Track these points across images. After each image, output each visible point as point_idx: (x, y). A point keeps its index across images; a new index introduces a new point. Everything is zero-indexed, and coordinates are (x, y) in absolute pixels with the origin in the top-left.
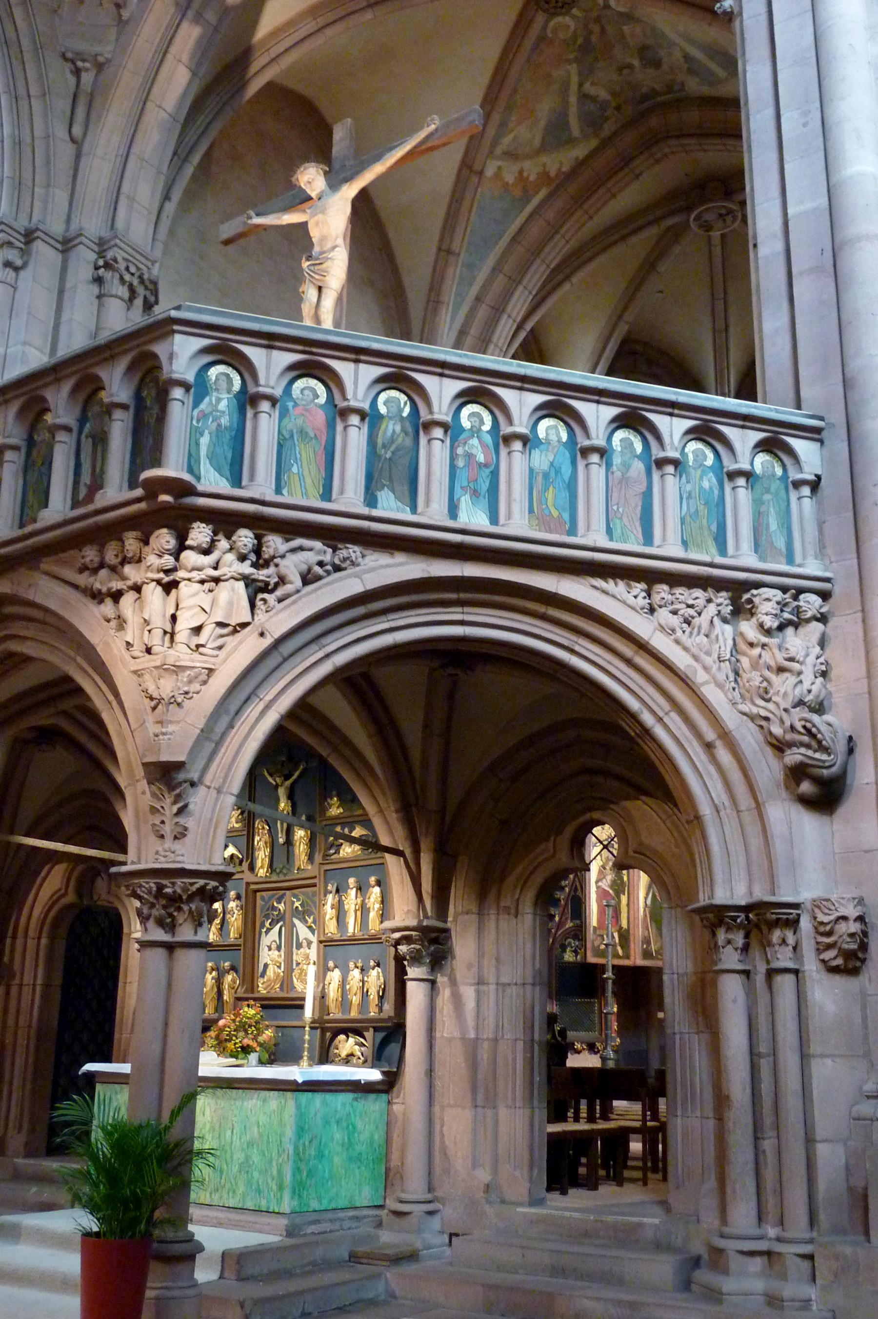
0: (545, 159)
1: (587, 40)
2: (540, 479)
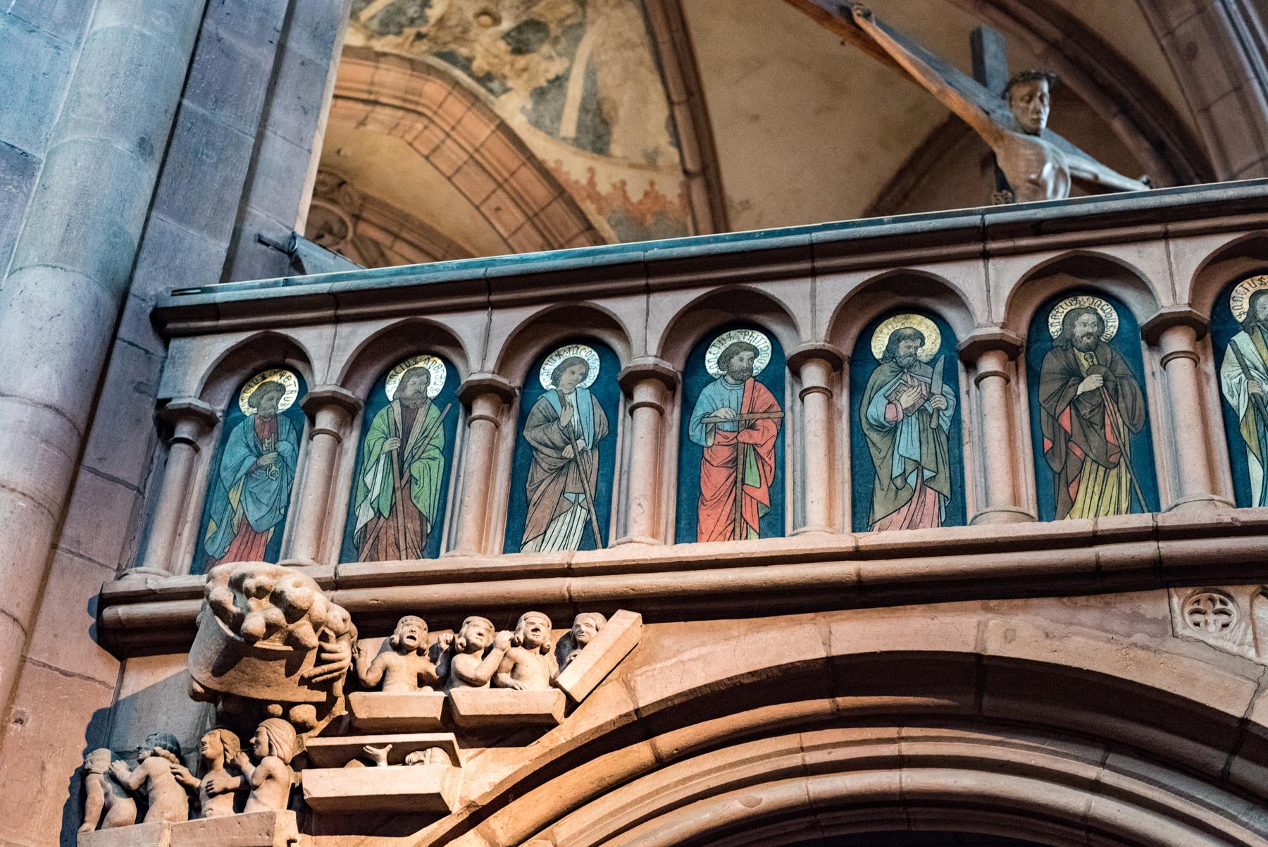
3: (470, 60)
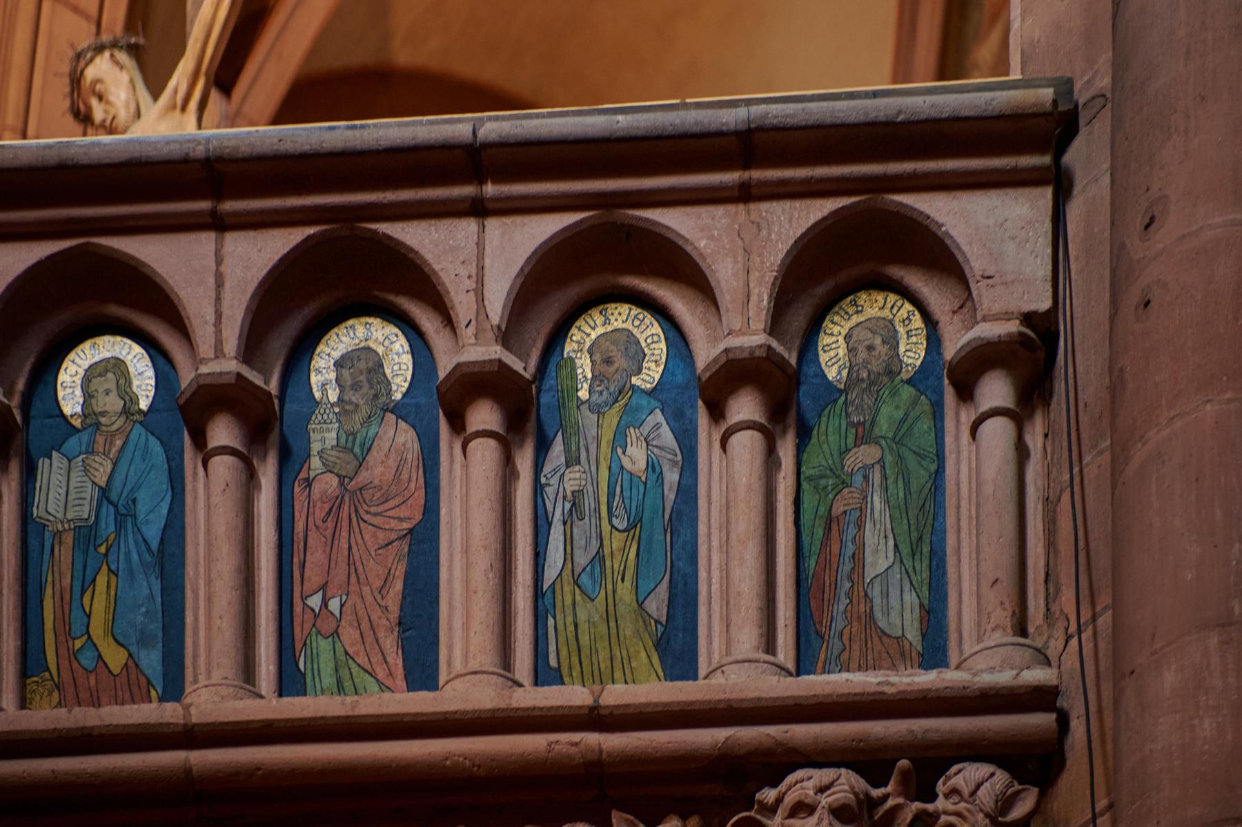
2: (65, 553)
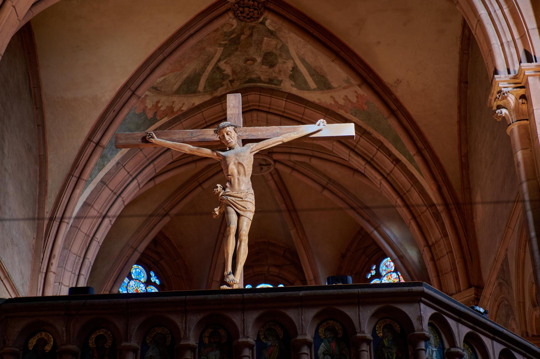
0: (175, 99)
1: (238, 37)
3: (259, 78)
